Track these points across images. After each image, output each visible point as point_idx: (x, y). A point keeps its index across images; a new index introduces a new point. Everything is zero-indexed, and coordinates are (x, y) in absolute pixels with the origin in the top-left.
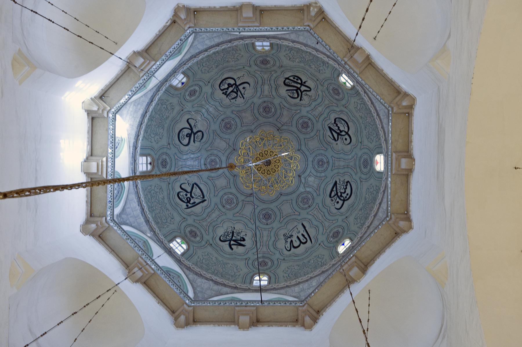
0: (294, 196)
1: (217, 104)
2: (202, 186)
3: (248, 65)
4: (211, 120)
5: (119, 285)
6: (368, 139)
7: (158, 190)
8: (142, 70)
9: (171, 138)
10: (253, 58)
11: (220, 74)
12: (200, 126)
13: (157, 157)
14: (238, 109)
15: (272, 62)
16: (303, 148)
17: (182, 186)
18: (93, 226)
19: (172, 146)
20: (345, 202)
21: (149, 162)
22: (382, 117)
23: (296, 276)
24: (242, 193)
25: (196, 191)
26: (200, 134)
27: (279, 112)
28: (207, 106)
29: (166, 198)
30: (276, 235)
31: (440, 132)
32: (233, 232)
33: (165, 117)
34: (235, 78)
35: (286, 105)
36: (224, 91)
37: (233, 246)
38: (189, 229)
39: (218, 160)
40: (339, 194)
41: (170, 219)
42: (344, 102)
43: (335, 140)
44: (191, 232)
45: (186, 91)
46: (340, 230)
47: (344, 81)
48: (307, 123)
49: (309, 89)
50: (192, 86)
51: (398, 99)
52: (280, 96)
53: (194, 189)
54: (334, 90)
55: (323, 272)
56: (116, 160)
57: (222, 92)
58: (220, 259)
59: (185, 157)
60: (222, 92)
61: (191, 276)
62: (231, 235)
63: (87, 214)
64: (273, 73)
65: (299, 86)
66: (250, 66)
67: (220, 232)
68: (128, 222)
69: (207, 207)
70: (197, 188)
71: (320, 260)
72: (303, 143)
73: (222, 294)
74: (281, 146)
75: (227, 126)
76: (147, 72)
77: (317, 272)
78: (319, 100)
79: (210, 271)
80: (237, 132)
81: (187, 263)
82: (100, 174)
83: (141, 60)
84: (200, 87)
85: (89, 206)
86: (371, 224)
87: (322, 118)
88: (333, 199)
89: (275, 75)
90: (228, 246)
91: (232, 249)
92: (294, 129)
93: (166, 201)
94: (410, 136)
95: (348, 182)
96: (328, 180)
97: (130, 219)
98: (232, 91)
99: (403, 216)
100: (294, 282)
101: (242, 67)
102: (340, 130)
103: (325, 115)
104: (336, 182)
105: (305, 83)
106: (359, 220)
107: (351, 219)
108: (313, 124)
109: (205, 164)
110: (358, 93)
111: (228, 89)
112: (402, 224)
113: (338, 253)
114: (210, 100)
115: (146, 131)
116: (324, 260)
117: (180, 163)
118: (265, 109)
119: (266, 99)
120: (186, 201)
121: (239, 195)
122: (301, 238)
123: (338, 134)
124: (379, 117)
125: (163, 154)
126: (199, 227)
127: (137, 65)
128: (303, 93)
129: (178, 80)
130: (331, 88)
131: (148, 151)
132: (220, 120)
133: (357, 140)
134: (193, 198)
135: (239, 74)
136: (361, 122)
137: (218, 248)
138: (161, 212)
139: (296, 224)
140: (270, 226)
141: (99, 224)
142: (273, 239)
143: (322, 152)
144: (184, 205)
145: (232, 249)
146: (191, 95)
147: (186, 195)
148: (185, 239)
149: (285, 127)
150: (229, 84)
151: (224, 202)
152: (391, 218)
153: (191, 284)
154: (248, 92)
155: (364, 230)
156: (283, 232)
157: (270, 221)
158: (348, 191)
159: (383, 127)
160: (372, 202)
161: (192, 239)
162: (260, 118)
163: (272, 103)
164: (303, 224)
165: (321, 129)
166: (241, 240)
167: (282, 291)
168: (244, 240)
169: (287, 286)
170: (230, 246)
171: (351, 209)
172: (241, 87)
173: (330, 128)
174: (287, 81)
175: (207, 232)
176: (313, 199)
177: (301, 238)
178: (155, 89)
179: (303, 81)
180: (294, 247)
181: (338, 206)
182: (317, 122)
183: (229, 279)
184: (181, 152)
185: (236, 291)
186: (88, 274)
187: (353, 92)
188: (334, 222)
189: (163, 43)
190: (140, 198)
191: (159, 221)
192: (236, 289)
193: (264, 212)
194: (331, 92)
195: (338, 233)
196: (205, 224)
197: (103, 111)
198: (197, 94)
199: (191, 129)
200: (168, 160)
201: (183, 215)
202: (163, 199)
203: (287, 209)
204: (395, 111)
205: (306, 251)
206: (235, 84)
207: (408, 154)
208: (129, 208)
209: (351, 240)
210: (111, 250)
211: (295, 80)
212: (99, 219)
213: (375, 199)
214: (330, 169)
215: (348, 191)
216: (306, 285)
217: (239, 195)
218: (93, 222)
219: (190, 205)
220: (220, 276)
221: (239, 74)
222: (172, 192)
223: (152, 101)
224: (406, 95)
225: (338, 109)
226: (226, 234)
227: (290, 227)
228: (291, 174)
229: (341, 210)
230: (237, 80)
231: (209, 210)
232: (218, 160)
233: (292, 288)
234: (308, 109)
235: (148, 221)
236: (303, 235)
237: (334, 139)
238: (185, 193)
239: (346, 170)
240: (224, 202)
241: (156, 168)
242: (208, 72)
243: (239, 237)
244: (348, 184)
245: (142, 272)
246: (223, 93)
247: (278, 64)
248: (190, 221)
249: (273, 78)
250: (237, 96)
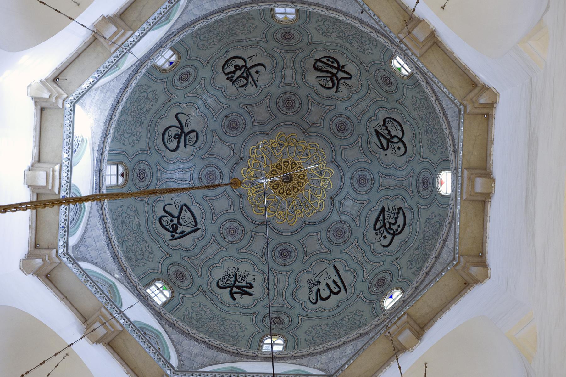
0: (324, 226)
1: (219, 93)
2: (193, 209)
3: (264, 39)
4: (210, 116)
5: (72, 347)
6: (430, 148)
7: (132, 213)
8: (114, 43)
9: (152, 139)
10: (272, 30)
11: (224, 51)
12: (194, 124)
13: (132, 165)
14: (247, 101)
15: (297, 37)
16: (338, 159)
17: (167, 208)
18: (39, 261)
19: (153, 151)
20: (396, 237)
21: (120, 173)
22: (450, 119)
23: (324, 340)
25: (186, 216)
26: (193, 135)
27: (305, 107)
28: (205, 96)
29: (143, 224)
30: (297, 281)
31: (532, 143)
32: (236, 275)
33: (145, 110)
34: (246, 58)
35: (316, 97)
36: (230, 76)
37: (235, 295)
38: (174, 269)
39: (217, 173)
40: (387, 226)
41: (147, 254)
42: (397, 96)
43: (384, 150)
44: (177, 273)
45: (176, 73)
46: (388, 276)
47: (399, 66)
48: (344, 124)
49: (349, 77)
50: (184, 67)
51: (473, 94)
52: (307, 85)
53: (183, 213)
54: (384, 78)
55: (362, 335)
56: (74, 168)
57: (227, 77)
58: (217, 312)
59: (171, 167)
60: (227, 77)
61: (175, 336)
62: (233, 279)
63: (30, 244)
64: (298, 52)
65: (335, 71)
66: (267, 42)
67: (218, 274)
68: (88, 256)
69: (200, 239)
70: (188, 211)
71: (358, 318)
72: (338, 152)
73: (218, 363)
74: (307, 155)
75: (232, 125)
76: (121, 46)
77: (354, 335)
78: (363, 93)
79: (201, 329)
80: (246, 133)
81: (169, 317)
82: (50, 188)
83: (113, 29)
84: (196, 69)
85: (34, 232)
86: (430, 269)
87: (365, 118)
88: (378, 231)
89: (301, 55)
90: (228, 294)
91: (234, 299)
92: (326, 132)
93: (143, 228)
94: (489, 147)
95: (400, 208)
96: (373, 204)
97: (91, 252)
98: (241, 76)
99: (476, 260)
100: (320, 348)
101: (255, 42)
102: (391, 135)
103: (370, 113)
104: (383, 209)
105: (343, 67)
106: (414, 263)
107: (403, 262)
108: (353, 126)
109: (199, 178)
110: (417, 84)
111: (234, 72)
112: (475, 270)
113: (383, 309)
114: (209, 88)
115: (117, 130)
116: (363, 318)
117: (165, 176)
118: (285, 102)
119: (288, 89)
120: (171, 230)
121: (245, 223)
122: (332, 286)
123: (389, 141)
124: (447, 119)
125: (140, 161)
126: (189, 267)
127: (108, 35)
128: (341, 82)
129: (165, 58)
130: (380, 75)
131: (120, 158)
132: (222, 116)
133: (415, 150)
134: (181, 225)
135: (251, 52)
136: (421, 125)
137: (214, 298)
138: (136, 244)
139: (325, 266)
140: (289, 268)
141: (47, 259)
142: (292, 285)
143: (365, 165)
144: (168, 235)
145: (234, 299)
146: (182, 80)
147: (172, 221)
148: (169, 283)
149: (313, 129)
150: (236, 66)
151: (225, 232)
152: (459, 262)
153: (175, 346)
154: (264, 78)
155: (420, 277)
156: (307, 276)
157: (288, 260)
158: (400, 221)
159: (451, 133)
160: (433, 238)
161: (179, 283)
162: (279, 115)
163: (296, 95)
164: (335, 267)
165: (364, 132)
166: (247, 287)
167: (303, 361)
168: (251, 287)
169: (311, 354)
170: (232, 294)
171: (403, 246)
172: (253, 71)
173: (376, 131)
174: (318, 63)
175: (199, 274)
176: (351, 231)
177: (332, 286)
178: (132, 69)
179: (341, 65)
180: (323, 299)
181: (386, 242)
182: (360, 122)
183: (228, 341)
184: (166, 160)
185: (238, 358)
186: (29, 329)
187: (411, 82)
188: (379, 265)
189: (144, 6)
190: (105, 223)
191: (133, 256)
192: (238, 356)
193: (281, 248)
194: (380, 81)
195: (384, 280)
196: (196, 262)
197: (56, 98)
198: (191, 78)
199: (182, 128)
200: (147, 171)
201: (166, 248)
202: (139, 225)
203: (313, 244)
204: (468, 111)
205: (339, 305)
206: (245, 66)
207: (484, 171)
208: (90, 237)
209: (403, 291)
210: (62, 297)
211: (330, 63)
212: (47, 252)
213: (437, 234)
214: (375, 189)
215: (400, 221)
216: (336, 354)
217: (245, 223)
218: (38, 256)
219: (176, 236)
220: (216, 336)
221: (251, 52)
222: (151, 216)
223: (127, 87)
224: (485, 88)
225: (389, 106)
226: (226, 277)
227: (317, 269)
228: (321, 196)
229: (389, 248)
230: (247, 61)
231: (204, 242)
232: (217, 173)
233: (318, 357)
234: (347, 104)
235: (117, 256)
236: (335, 282)
237: (383, 147)
238: (170, 218)
239: (397, 192)
240: (225, 232)
241: (130, 182)
242: (207, 48)
243: (245, 282)
244: (401, 211)
245: (106, 328)
246: (228, 78)
247: (306, 40)
248: (176, 258)
249: (298, 59)
250: (246, 84)
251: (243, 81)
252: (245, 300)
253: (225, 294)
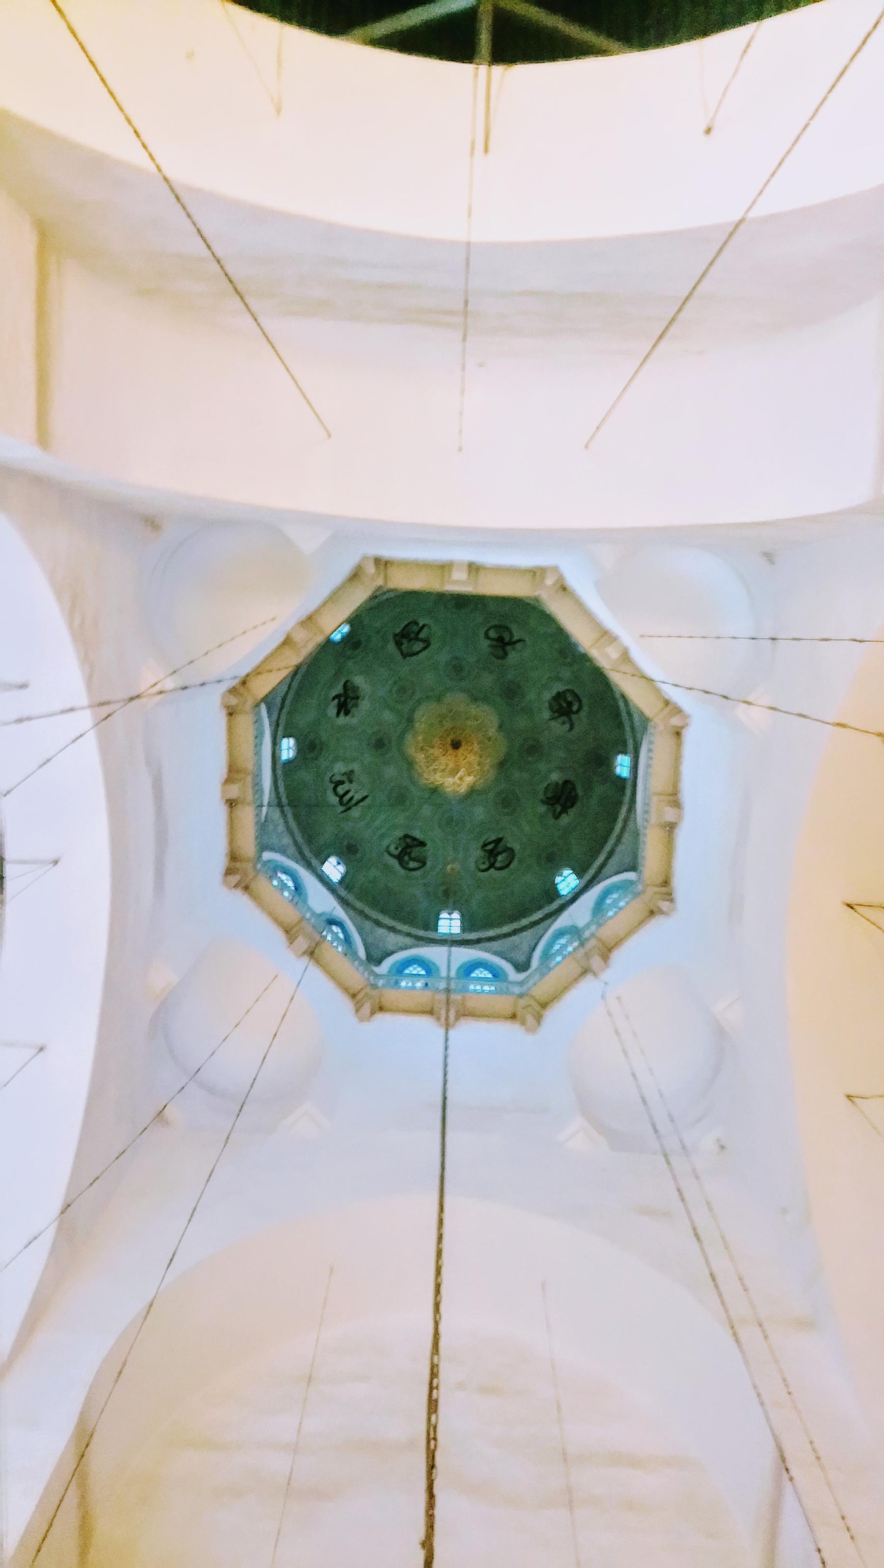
2: (425, 653)
12: (513, 656)
24: (412, 711)
25: (421, 645)
37: (336, 701)
65: (562, 801)
67: (359, 680)
91: (334, 699)
95: (424, 864)
98: (561, 706)
123: (491, 852)
144: (398, 631)
145: (334, 699)
154: (559, 728)
164: (366, 797)
180: (335, 789)
181: (392, 849)
203: (390, 772)
215: (412, 864)
226: (355, 689)
236: (351, 798)
237: (485, 845)
251: (556, 707)
252: (332, 710)
253: (338, 689)
